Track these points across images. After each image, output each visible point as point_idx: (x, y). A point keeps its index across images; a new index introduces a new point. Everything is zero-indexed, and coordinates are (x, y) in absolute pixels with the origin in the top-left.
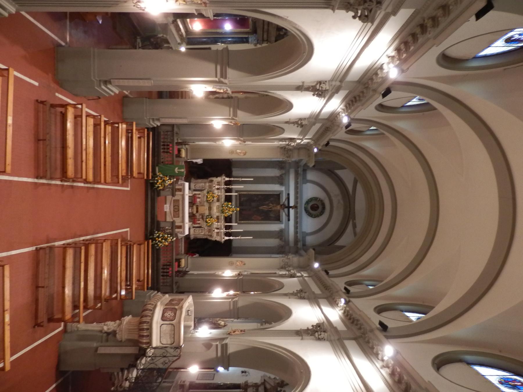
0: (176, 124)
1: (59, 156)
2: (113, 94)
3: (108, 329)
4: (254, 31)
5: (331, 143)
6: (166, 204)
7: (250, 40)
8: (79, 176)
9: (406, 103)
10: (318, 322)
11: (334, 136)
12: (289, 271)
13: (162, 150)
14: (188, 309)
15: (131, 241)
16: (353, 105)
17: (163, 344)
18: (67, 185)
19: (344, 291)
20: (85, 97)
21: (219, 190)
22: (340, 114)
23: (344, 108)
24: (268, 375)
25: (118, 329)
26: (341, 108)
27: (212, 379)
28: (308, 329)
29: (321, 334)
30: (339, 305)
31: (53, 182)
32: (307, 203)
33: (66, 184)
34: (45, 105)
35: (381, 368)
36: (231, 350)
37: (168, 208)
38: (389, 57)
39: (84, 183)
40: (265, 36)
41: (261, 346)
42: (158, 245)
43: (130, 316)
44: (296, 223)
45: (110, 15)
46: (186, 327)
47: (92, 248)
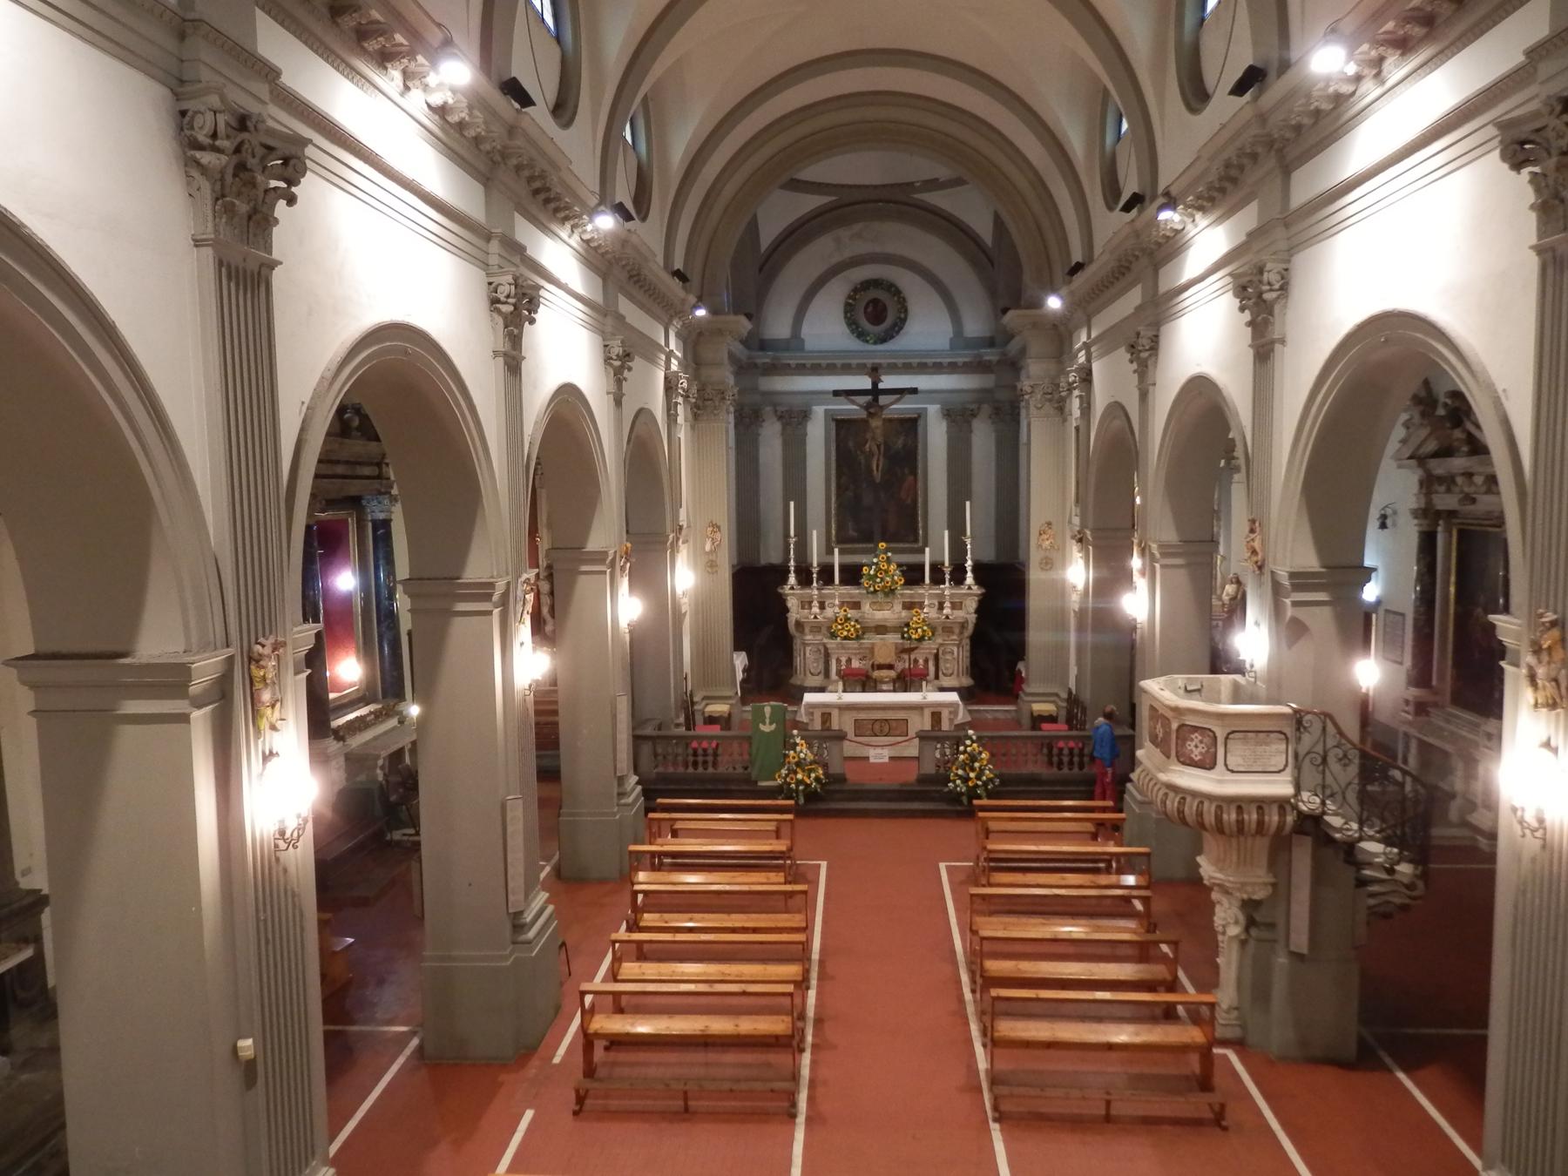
0: (634, 729)
1: (730, 1057)
2: (550, 908)
3: (1236, 922)
4: (355, 502)
5: (678, 264)
6: (867, 758)
7: (381, 516)
8: (787, 1001)
9: (548, 29)
10: (1231, 293)
11: (656, 256)
12: (1070, 390)
13: (711, 770)
14: (1182, 692)
15: (978, 858)
16: (558, 198)
17: (1286, 765)
18: (814, 1036)
19: (1134, 212)
20: (562, 984)
22: (587, 237)
23: (568, 226)
24: (1393, 446)
25: (1238, 894)
26: (570, 237)
27: (1398, 617)
28: (1251, 324)
29: (1269, 284)
30: (1179, 227)
31: (805, 1072)
32: (861, 335)
33: (809, 1038)
34: (587, 1091)
35: (1383, 83)
36: (1309, 561)
37: (879, 751)
38: (407, 88)
39: (808, 988)
40: (367, 471)
41: (1299, 470)
42: (990, 780)
43: (1199, 859)
44: (923, 368)
45: (328, 916)
46: (1238, 696)
47: (996, 966)
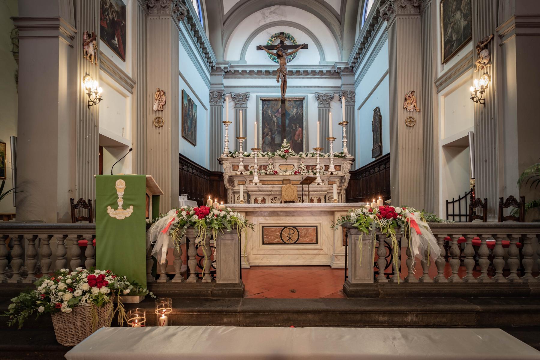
21: (249, 167)
